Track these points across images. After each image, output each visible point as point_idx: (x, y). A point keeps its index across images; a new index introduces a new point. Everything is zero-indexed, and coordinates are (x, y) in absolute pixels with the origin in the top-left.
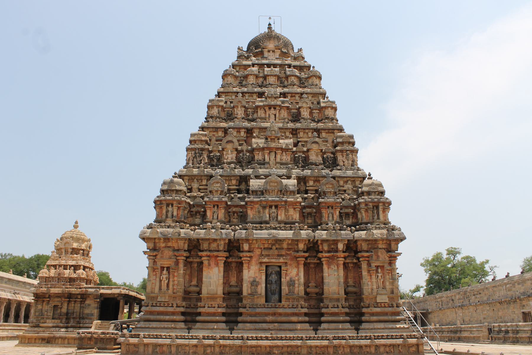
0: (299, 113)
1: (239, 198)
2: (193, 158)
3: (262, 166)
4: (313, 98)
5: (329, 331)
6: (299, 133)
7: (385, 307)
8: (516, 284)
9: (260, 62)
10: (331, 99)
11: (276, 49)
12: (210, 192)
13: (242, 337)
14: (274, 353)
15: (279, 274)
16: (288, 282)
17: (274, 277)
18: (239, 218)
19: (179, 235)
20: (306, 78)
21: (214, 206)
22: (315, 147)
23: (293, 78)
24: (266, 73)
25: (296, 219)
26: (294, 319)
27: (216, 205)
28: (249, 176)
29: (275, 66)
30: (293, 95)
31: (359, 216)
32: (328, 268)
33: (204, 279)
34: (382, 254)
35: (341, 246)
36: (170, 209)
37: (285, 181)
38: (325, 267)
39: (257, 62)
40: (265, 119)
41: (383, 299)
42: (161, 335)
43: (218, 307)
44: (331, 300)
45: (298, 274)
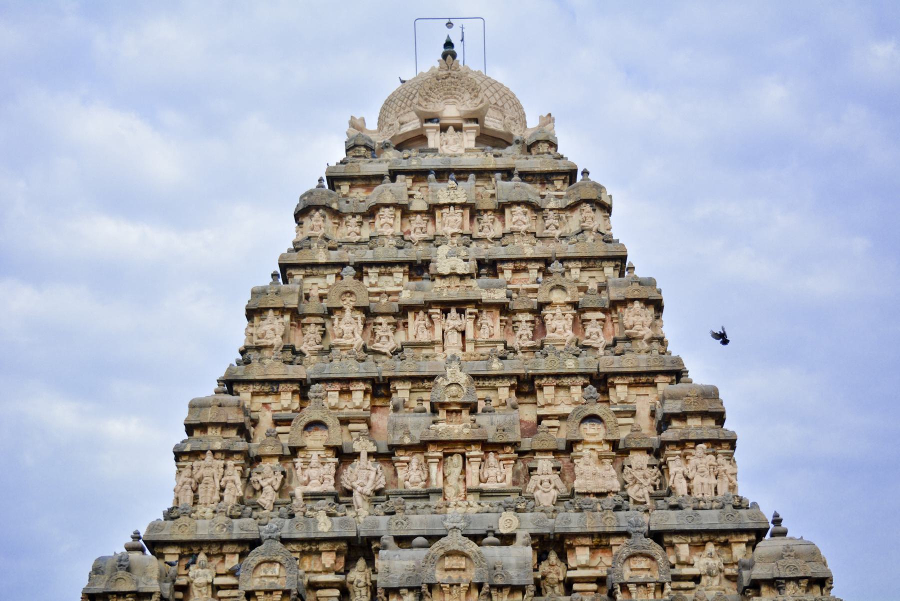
3: (421, 503)
4: (586, 275)
6: (541, 388)
10: (640, 273)
22: (591, 431)
23: (518, 209)
28: (378, 539)
29: (461, 174)
37: (494, 553)
39: (404, 165)
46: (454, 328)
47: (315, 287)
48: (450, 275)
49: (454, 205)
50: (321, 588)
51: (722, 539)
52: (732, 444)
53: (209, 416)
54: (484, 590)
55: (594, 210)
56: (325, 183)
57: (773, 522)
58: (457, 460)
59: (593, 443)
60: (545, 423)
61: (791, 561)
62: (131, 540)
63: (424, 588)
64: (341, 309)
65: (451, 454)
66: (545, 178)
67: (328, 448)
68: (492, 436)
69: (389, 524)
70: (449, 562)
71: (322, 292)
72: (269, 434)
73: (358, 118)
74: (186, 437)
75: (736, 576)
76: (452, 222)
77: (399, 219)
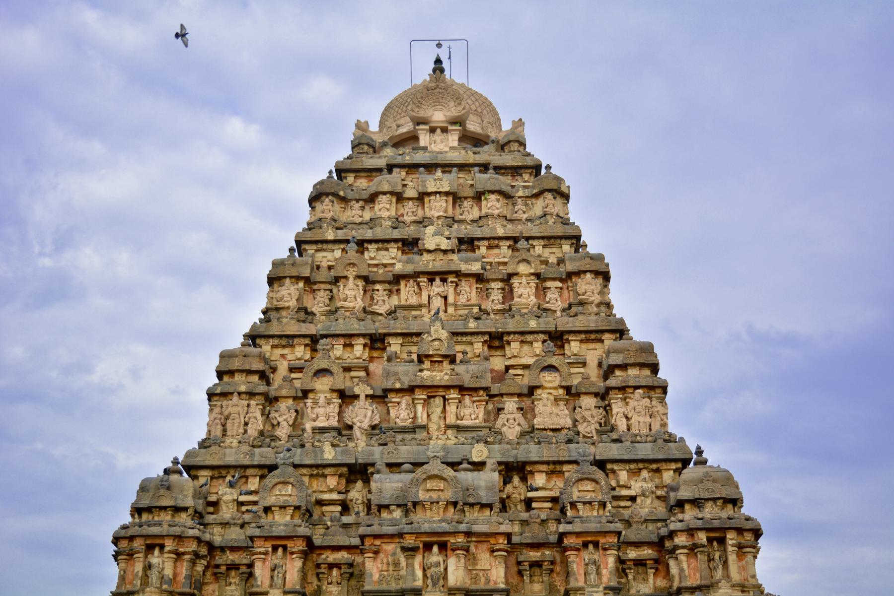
3: (408, 436)
6: (509, 343)
9: (408, 159)
10: (592, 249)
12: (267, 510)
18: (344, 583)
21: (275, 548)
22: (550, 379)
23: (493, 197)
27: (279, 543)
28: (373, 465)
29: (446, 167)
36: (155, 559)
37: (467, 477)
39: (399, 160)
40: (419, 307)
46: (438, 294)
47: (325, 260)
48: (436, 250)
49: (440, 193)
50: (326, 505)
51: (654, 466)
52: (664, 389)
53: (236, 364)
54: (459, 507)
55: (555, 198)
56: (334, 175)
57: (696, 453)
58: (438, 401)
59: (551, 388)
60: (511, 371)
61: (709, 485)
62: (171, 465)
63: (410, 505)
64: (346, 277)
65: (434, 397)
66: (515, 171)
68: (467, 382)
69: (382, 453)
70: (429, 485)
71: (330, 263)
72: (285, 379)
73: (363, 121)
74: (217, 381)
75: (665, 497)
76: (437, 207)
77: (394, 205)
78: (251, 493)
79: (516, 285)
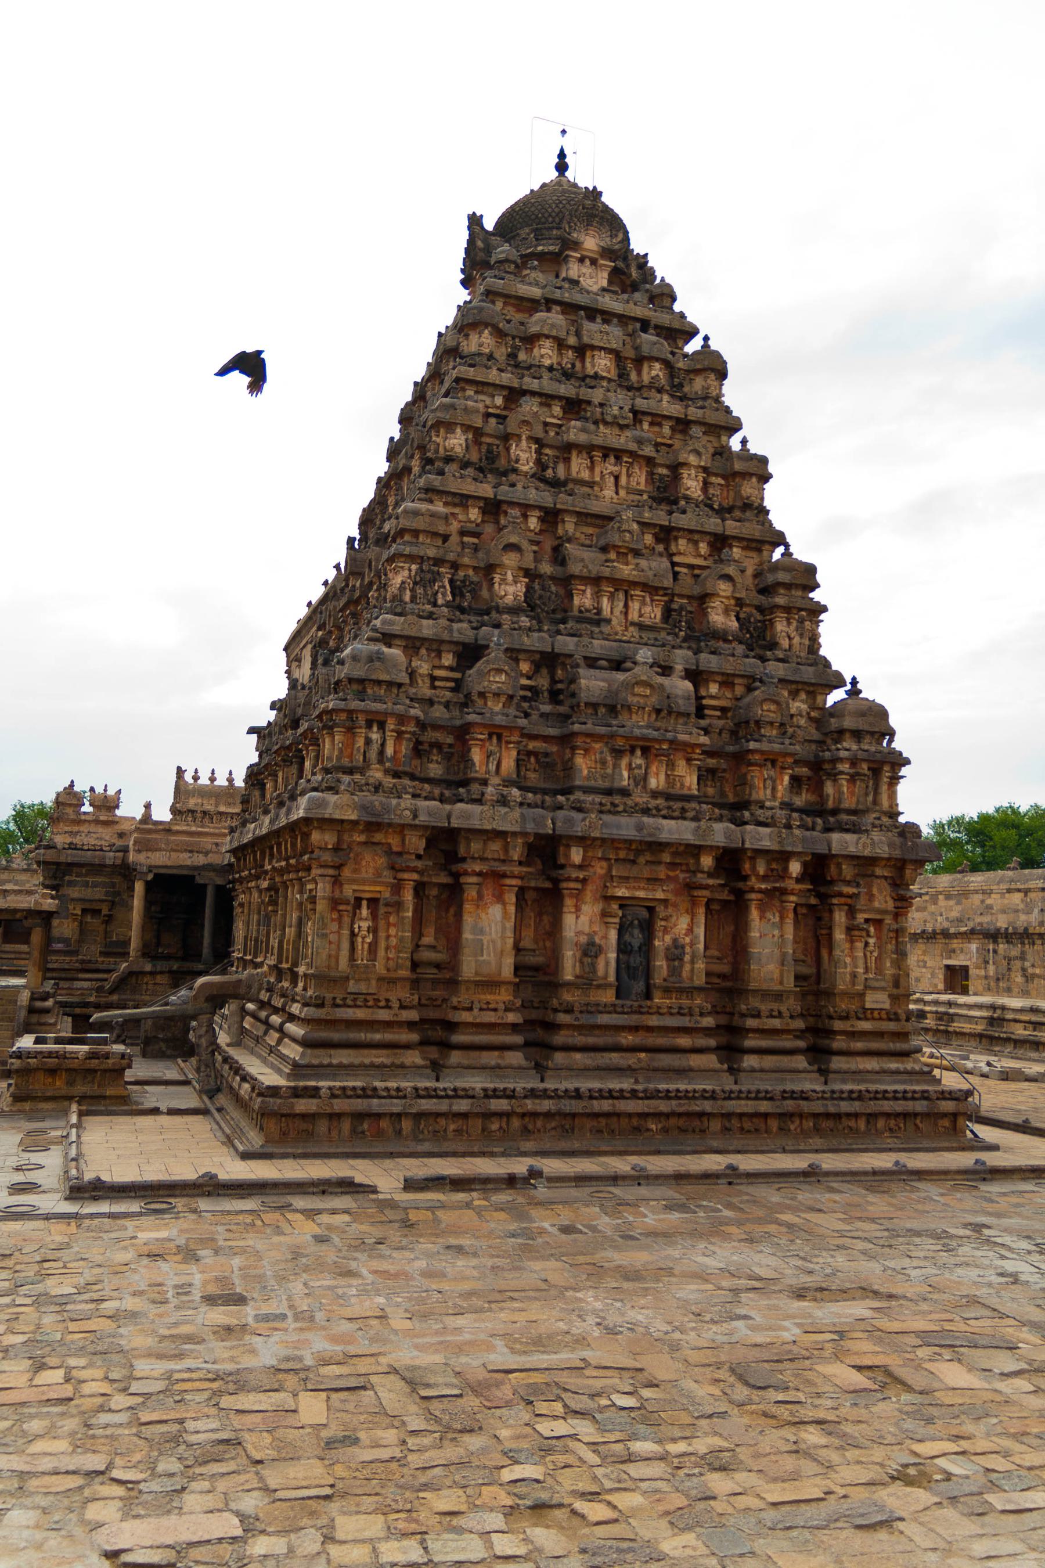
0: (676, 477)
1: (542, 715)
2: (415, 583)
5: (763, 1075)
6: (676, 539)
7: (881, 1019)
8: (941, 897)
11: (602, 257)
13: (577, 1090)
14: (648, 1130)
15: (648, 928)
16: (667, 949)
17: (636, 938)
19: (415, 816)
20: (688, 372)
21: (490, 735)
23: (657, 365)
24: (586, 340)
25: (689, 789)
26: (684, 1041)
27: (497, 733)
30: (657, 420)
31: (829, 789)
32: (762, 917)
33: (467, 935)
34: (880, 891)
35: (795, 868)
38: (754, 914)
40: (591, 484)
41: (878, 1000)
42: (375, 1089)
43: (507, 1010)
44: (765, 994)
45: (690, 931)
46: (611, 473)
61: (871, 719)
67: (520, 568)
69: (577, 645)
78: (440, 667)
79: (685, 476)
